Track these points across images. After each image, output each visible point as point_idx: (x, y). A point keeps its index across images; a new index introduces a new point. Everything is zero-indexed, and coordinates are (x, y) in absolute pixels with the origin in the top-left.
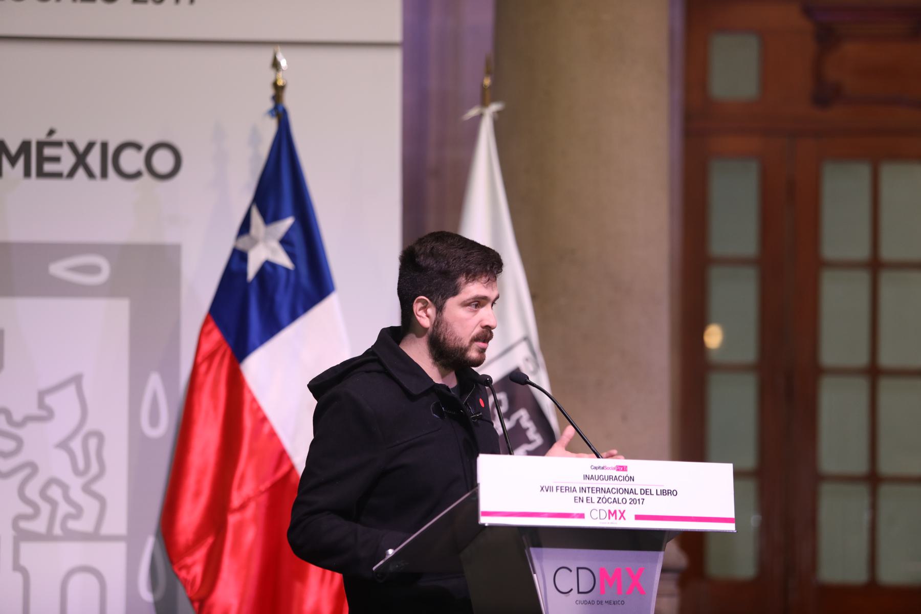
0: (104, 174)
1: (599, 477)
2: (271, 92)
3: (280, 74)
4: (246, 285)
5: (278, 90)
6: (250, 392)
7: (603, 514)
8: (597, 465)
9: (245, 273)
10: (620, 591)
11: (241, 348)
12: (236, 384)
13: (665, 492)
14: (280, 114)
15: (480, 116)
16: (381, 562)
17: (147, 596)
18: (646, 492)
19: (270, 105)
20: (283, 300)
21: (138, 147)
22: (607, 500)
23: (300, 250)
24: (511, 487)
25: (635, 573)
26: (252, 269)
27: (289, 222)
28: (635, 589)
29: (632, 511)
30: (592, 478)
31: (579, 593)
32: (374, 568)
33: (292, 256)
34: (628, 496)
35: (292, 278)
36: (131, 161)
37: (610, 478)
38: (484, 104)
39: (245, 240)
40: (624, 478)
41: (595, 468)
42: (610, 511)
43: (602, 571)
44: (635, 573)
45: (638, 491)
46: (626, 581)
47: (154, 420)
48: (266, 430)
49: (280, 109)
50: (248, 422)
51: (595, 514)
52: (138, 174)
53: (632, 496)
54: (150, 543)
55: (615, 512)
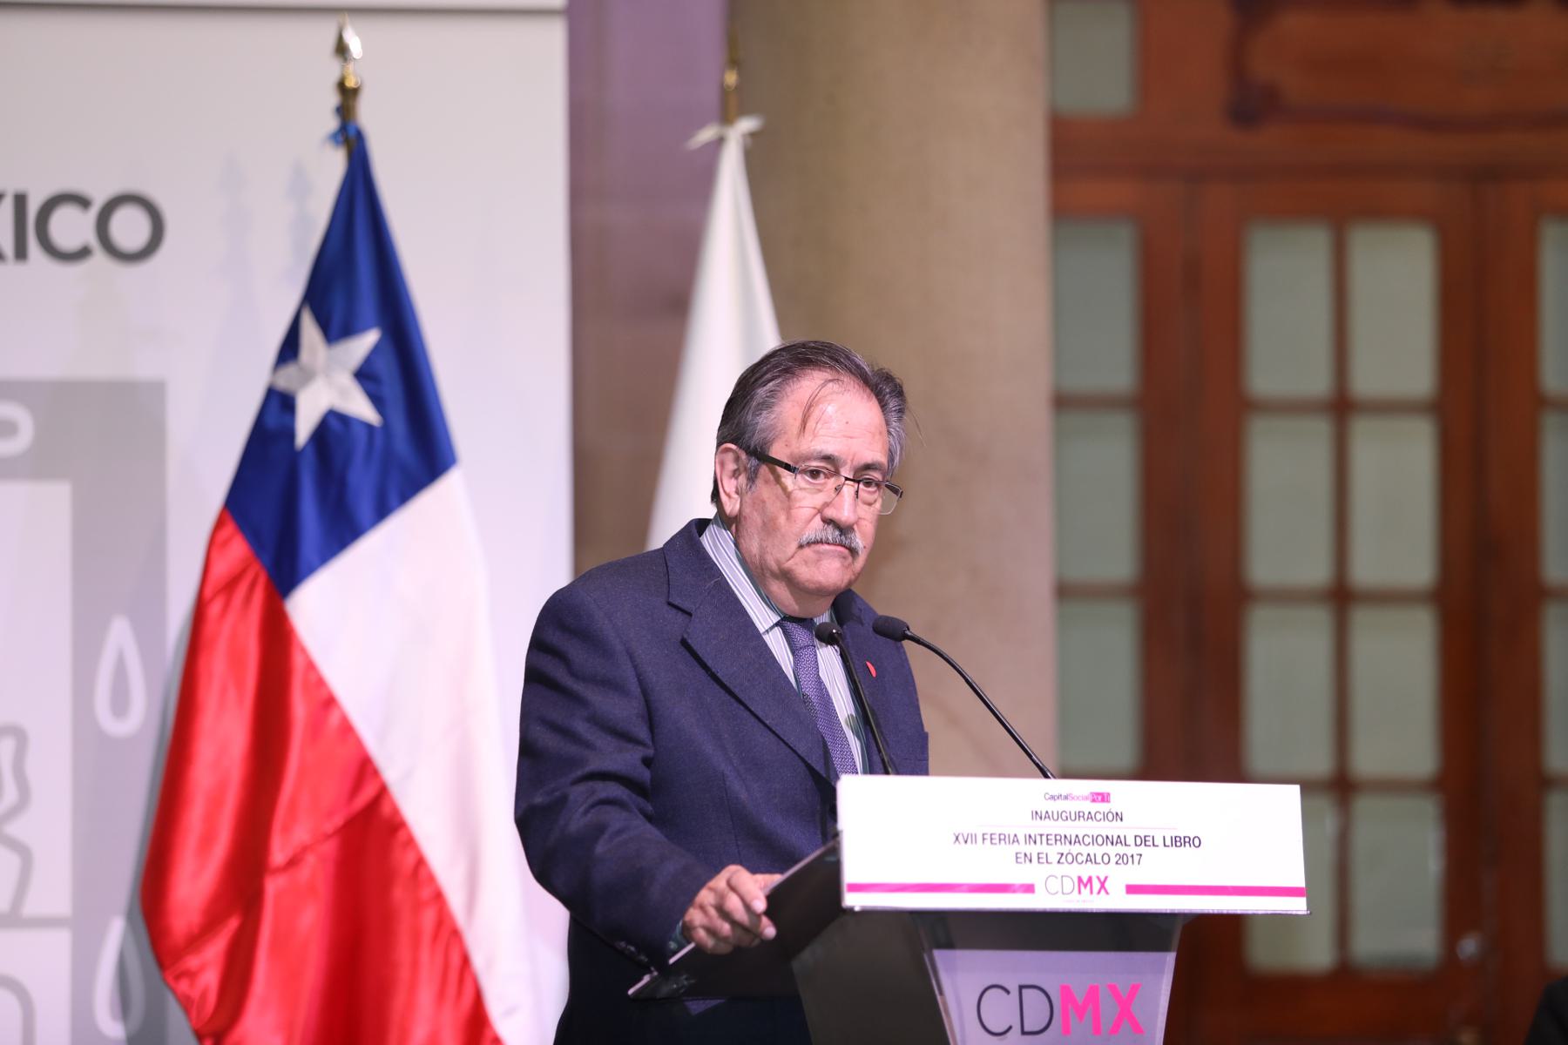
0: (21, 253)
1: (1060, 815)
2: (333, 99)
3: (351, 67)
4: (294, 456)
5: (348, 95)
6: (304, 651)
7: (1068, 885)
8: (1056, 793)
9: (290, 434)
10: (1097, 1030)
11: (285, 572)
12: (277, 637)
13: (1178, 842)
14: (352, 140)
15: (720, 142)
16: (646, 979)
17: (112, 1028)
18: (1144, 841)
19: (332, 124)
20: (362, 482)
21: (83, 202)
22: (1075, 859)
23: (393, 389)
24: (904, 839)
25: (1124, 991)
26: (304, 427)
27: (369, 339)
28: (1126, 1026)
29: (1120, 876)
30: (1047, 816)
31: (1024, 1033)
32: (631, 992)
33: (377, 400)
34: (1113, 850)
35: (379, 441)
36: (71, 228)
37: (1079, 815)
38: (726, 119)
39: (290, 370)
40: (1105, 817)
41: (1053, 797)
42: (1080, 879)
43: (1066, 991)
44: (1124, 994)
45: (1130, 841)
46: (1109, 1009)
47: (120, 705)
48: (334, 720)
49: (352, 133)
50: (300, 709)
51: (1054, 885)
52: (83, 253)
53: (1120, 849)
54: (116, 934)
55: (1090, 879)
